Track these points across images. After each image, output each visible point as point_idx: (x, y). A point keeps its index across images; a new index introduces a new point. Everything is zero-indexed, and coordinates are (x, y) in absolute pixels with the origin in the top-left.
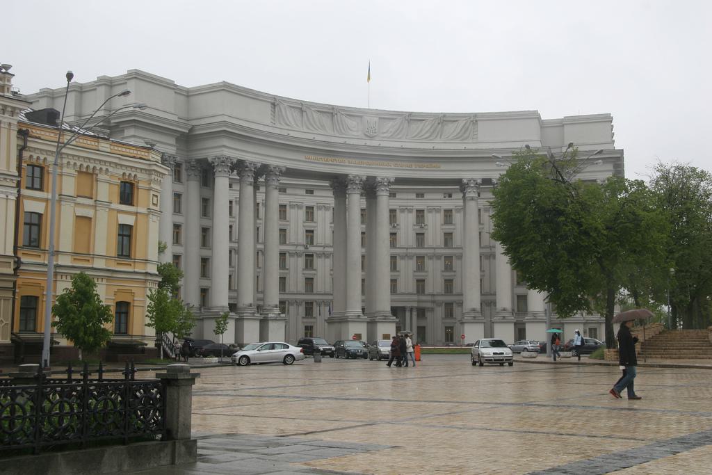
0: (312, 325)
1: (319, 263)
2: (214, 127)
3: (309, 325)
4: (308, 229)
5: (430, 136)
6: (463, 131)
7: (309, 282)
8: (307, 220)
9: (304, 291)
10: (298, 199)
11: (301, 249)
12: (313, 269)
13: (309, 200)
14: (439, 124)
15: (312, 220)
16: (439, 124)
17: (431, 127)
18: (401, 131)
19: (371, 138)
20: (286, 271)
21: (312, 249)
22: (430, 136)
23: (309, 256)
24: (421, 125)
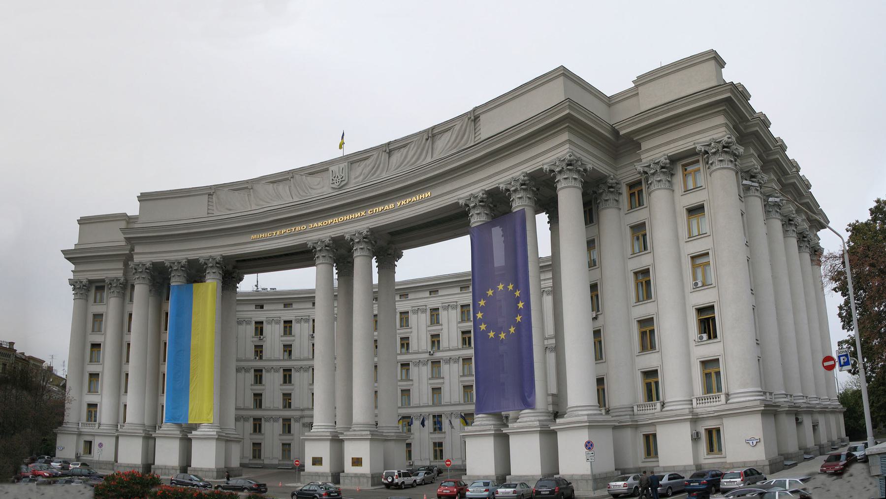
0: (440, 441)
1: (445, 368)
2: (193, 228)
3: (437, 441)
4: (433, 333)
5: (418, 159)
6: (461, 133)
7: (436, 391)
8: (432, 323)
9: (431, 403)
10: (421, 303)
11: (427, 355)
12: (440, 378)
13: (434, 302)
14: (427, 139)
15: (438, 323)
16: (427, 139)
17: (418, 148)
18: (379, 166)
19: (340, 188)
20: (410, 383)
21: (438, 355)
22: (418, 159)
23: (436, 363)
24: (404, 151)
